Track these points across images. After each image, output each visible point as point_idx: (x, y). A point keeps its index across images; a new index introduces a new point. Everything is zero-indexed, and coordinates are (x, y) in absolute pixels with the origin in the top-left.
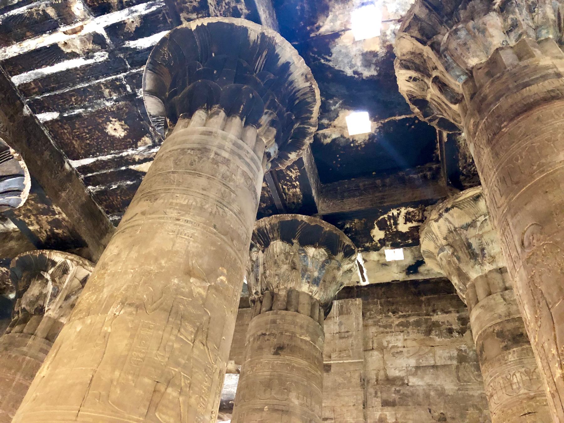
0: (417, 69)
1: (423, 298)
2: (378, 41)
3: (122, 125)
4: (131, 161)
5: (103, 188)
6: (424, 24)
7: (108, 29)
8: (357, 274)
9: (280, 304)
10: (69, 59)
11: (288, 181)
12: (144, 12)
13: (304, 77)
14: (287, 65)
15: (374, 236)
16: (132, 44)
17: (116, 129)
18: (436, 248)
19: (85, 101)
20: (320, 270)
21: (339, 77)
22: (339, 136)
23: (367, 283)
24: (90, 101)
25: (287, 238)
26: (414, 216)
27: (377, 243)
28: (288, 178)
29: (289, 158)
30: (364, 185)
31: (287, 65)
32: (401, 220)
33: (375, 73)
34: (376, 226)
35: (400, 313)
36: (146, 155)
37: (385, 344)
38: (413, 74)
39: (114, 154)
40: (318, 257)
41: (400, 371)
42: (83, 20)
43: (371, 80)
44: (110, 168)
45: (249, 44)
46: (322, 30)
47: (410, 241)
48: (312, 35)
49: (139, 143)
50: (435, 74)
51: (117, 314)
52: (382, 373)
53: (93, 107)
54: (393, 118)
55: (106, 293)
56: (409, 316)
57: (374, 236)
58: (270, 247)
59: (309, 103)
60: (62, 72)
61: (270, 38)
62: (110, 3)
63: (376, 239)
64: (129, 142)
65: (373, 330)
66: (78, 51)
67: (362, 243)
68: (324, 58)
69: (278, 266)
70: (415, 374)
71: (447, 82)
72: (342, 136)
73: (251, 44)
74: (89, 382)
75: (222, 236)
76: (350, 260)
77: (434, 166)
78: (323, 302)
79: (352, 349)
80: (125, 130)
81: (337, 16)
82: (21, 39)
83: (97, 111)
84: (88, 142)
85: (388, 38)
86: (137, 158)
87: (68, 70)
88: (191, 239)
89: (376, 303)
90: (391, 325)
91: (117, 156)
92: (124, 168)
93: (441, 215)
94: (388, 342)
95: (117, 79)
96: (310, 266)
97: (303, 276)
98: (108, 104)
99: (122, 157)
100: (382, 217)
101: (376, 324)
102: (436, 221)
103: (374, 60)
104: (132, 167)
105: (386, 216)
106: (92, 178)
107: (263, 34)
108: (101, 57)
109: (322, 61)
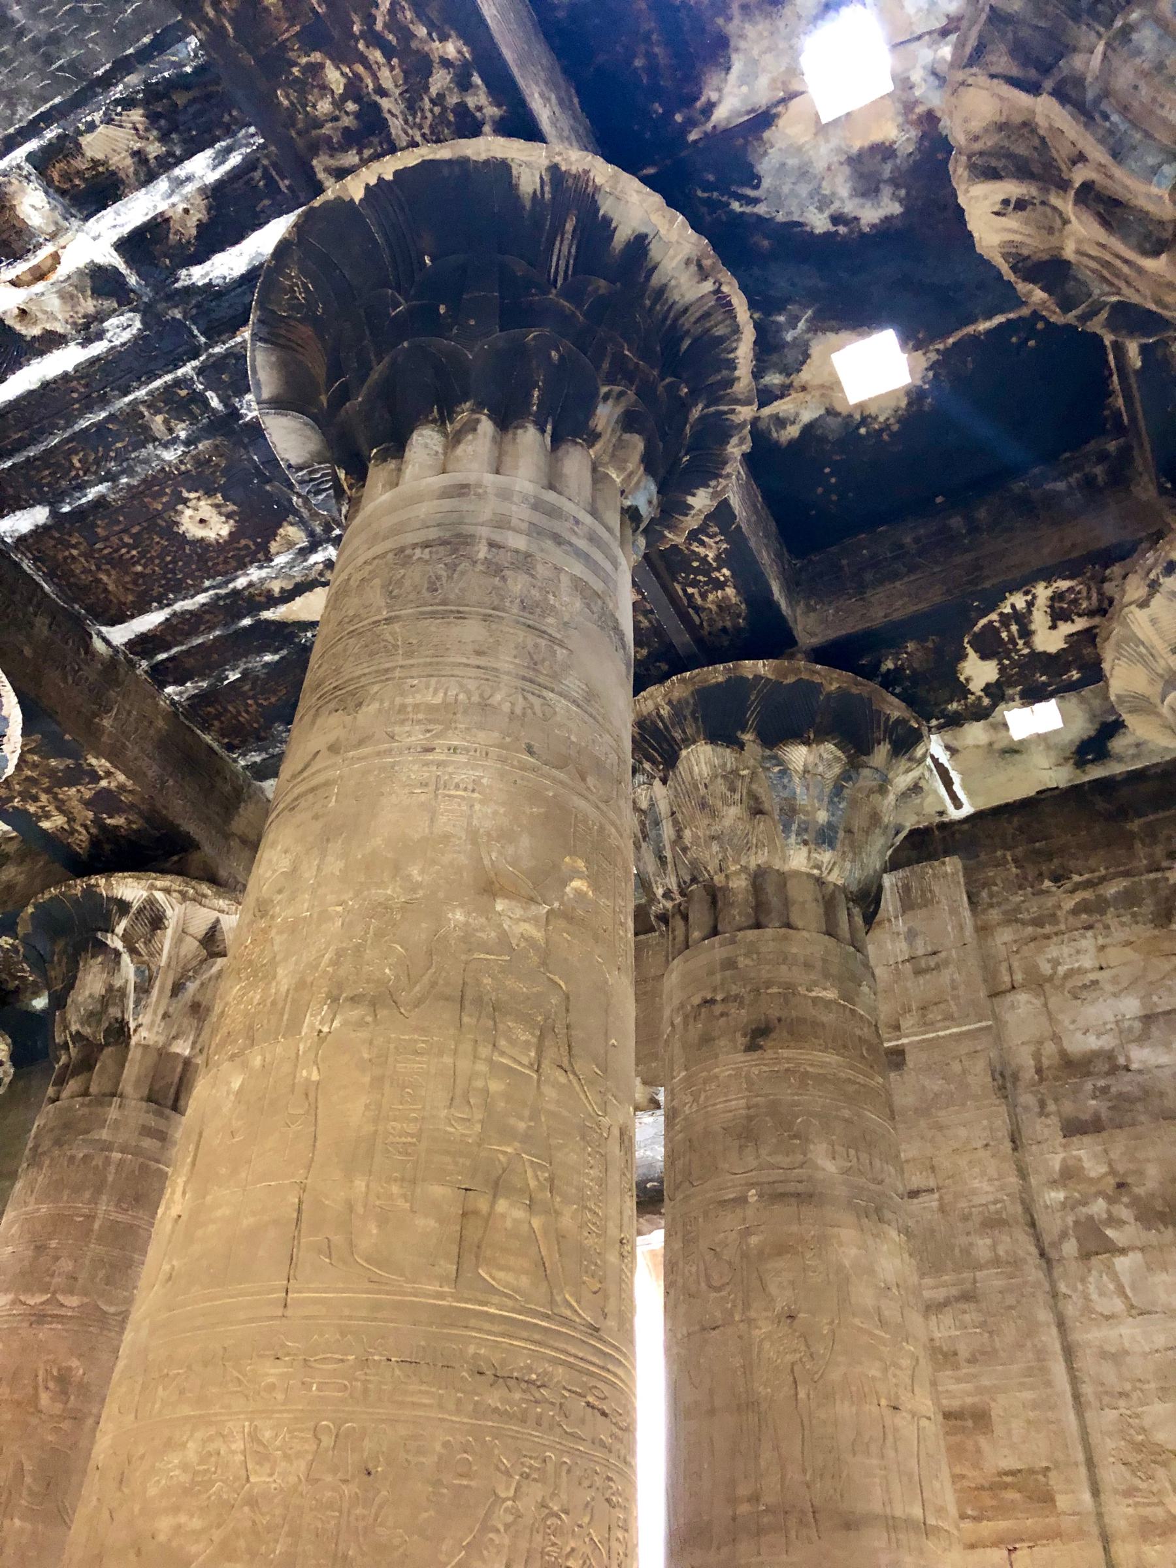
0: (1023, 171)
1: (1135, 825)
2: (892, 109)
3: (217, 506)
4: (263, 599)
5: (205, 684)
6: (1025, 33)
8: (935, 792)
9: (737, 914)
10: (41, 353)
11: (697, 571)
12: (212, 177)
13: (693, 268)
14: (640, 244)
15: (967, 680)
16: (197, 275)
17: (204, 521)
18: (1152, 682)
19: (107, 459)
20: (831, 802)
21: (793, 241)
22: (822, 411)
23: (967, 810)
24: (120, 458)
25: (722, 732)
26: (1075, 602)
27: (980, 698)
28: (695, 564)
29: (691, 507)
30: (917, 540)
31: (640, 244)
32: (1040, 619)
33: (896, 209)
34: (970, 650)
35: (1076, 878)
37: (1046, 969)
38: (1012, 189)
40: (821, 769)
41: (1099, 1035)
42: (53, 237)
43: (886, 232)
44: (211, 629)
45: (524, 207)
46: (720, 115)
47: (1075, 675)
48: (693, 136)
49: (274, 547)
50: (1079, 176)
51: (325, 1029)
52: (1050, 1048)
53: (130, 472)
54: (970, 329)
55: (284, 978)
56: (1103, 879)
57: (967, 680)
58: (682, 766)
59: (721, 340)
60: (31, 393)
61: (576, 177)
62: (113, 173)
63: (976, 686)
64: (247, 547)
65: (1005, 936)
66: (59, 328)
67: (937, 704)
68: (740, 198)
69: (714, 814)
70: (1143, 1038)
71: (1122, 194)
72: (831, 412)
73: (528, 205)
74: (295, 1215)
75: (555, 772)
76: (910, 759)
77: (1112, 446)
78: (854, 888)
79: (956, 998)
80: (229, 516)
81: (756, 62)
83: (144, 481)
84: (139, 568)
85: (917, 93)
86: (276, 587)
87: (45, 385)
88: (476, 795)
89: (1000, 863)
90: (1054, 915)
91: (222, 592)
92: (247, 622)
93: (1154, 586)
94: (1056, 963)
95: (177, 383)
96: (803, 798)
97: (787, 828)
98: (170, 455)
99: (236, 593)
100: (983, 622)
101: (1012, 918)
102: (1144, 604)
103: (887, 170)
104: (268, 615)
105: (994, 616)
106: (170, 665)
107: (554, 169)
108: (122, 329)
109: (736, 206)
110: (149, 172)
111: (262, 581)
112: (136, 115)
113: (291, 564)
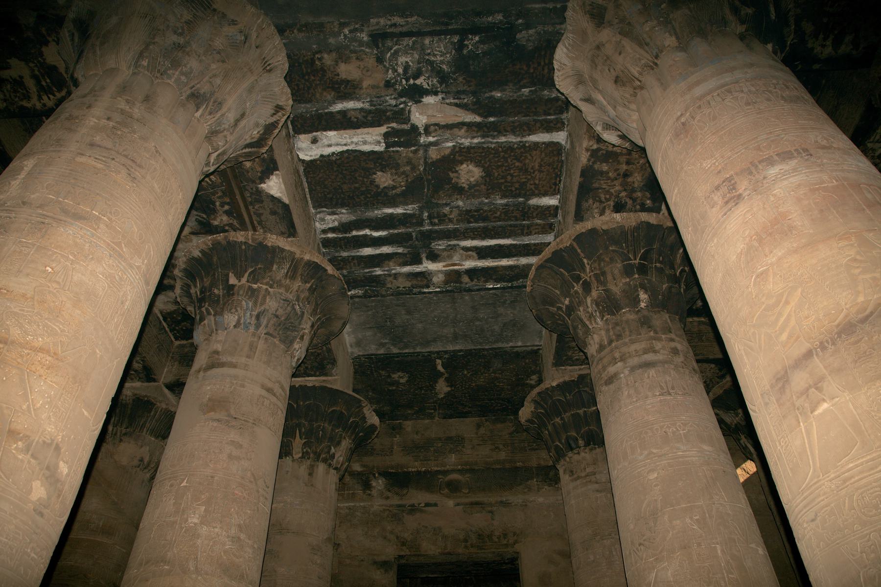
4: (474, 128)
7: (420, 262)
16: (400, 250)
36: (447, 135)
39: (491, 143)
44: (513, 122)
49: (447, 152)
64: (460, 156)
66: (461, 251)
82: (511, 267)
84: (517, 164)
91: (490, 140)
92: (492, 119)
98: (460, 203)
99: (483, 137)
104: (478, 119)
108: (440, 245)
110: (396, 276)
111: (466, 138)
112: (389, 286)
113: (447, 140)
